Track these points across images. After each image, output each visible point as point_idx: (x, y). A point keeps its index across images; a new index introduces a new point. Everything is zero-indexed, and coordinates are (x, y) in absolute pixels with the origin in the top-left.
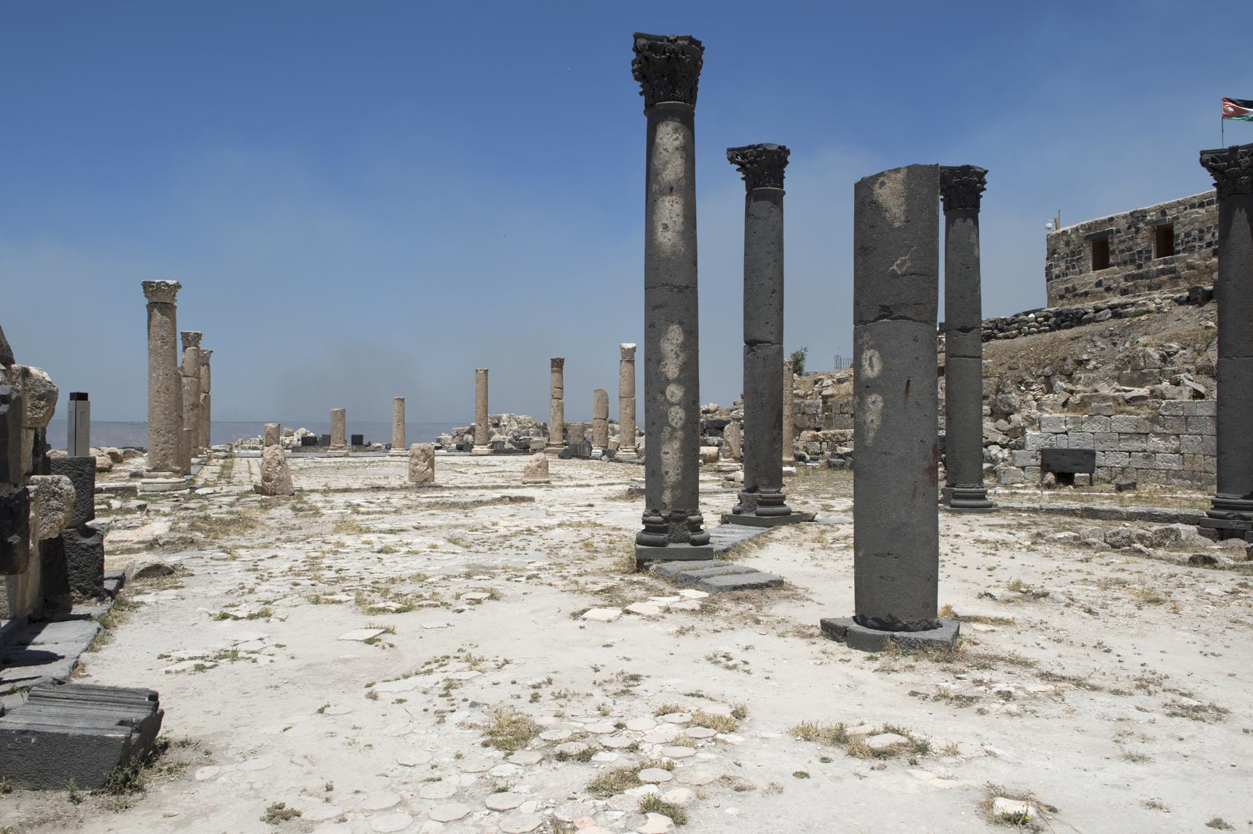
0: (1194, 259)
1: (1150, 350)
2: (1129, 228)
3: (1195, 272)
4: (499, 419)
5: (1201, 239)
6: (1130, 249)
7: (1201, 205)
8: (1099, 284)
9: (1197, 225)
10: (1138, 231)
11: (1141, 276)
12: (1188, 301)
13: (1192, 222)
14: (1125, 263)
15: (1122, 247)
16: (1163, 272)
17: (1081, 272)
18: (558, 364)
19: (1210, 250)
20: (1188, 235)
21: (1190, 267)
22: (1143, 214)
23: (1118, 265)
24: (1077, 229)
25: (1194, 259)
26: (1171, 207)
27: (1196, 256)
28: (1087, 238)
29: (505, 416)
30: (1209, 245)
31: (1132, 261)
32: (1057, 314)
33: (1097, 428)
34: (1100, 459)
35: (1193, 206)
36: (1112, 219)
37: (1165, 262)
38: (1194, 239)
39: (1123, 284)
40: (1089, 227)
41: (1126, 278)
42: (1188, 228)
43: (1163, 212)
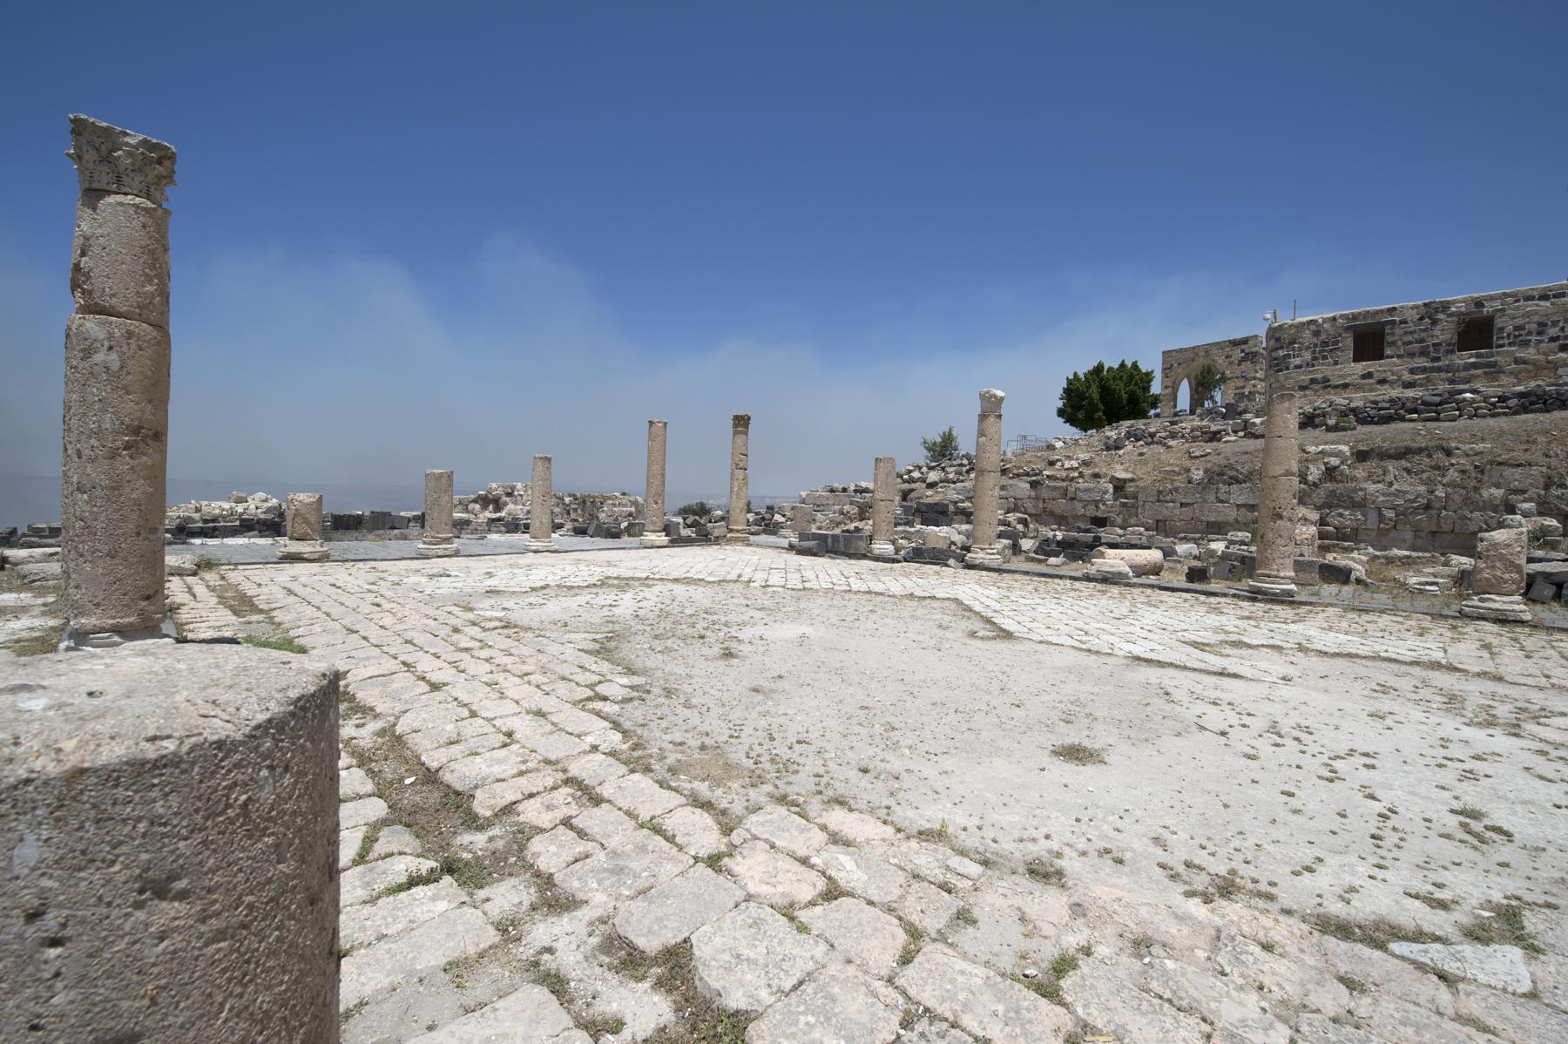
0: (1530, 353)
2: (1422, 318)
3: (1530, 367)
4: (513, 488)
5: (1539, 333)
6: (1422, 341)
7: (1544, 297)
8: (1364, 377)
9: (1536, 318)
10: (1435, 322)
11: (1439, 370)
13: (1528, 315)
14: (1412, 355)
15: (1410, 338)
16: (1474, 366)
17: (1336, 363)
18: (742, 422)
19: (1555, 345)
20: (1516, 328)
22: (1445, 306)
23: (1399, 357)
24: (1334, 319)
26: (1491, 298)
27: (1532, 350)
28: (1348, 328)
29: (519, 485)
30: (1553, 339)
31: (1424, 353)
32: (1521, 395)
35: (1530, 298)
36: (1394, 309)
37: (1478, 356)
38: (1530, 333)
39: (1407, 377)
40: (1355, 317)
41: (1412, 371)
42: (1519, 322)
43: (1479, 304)
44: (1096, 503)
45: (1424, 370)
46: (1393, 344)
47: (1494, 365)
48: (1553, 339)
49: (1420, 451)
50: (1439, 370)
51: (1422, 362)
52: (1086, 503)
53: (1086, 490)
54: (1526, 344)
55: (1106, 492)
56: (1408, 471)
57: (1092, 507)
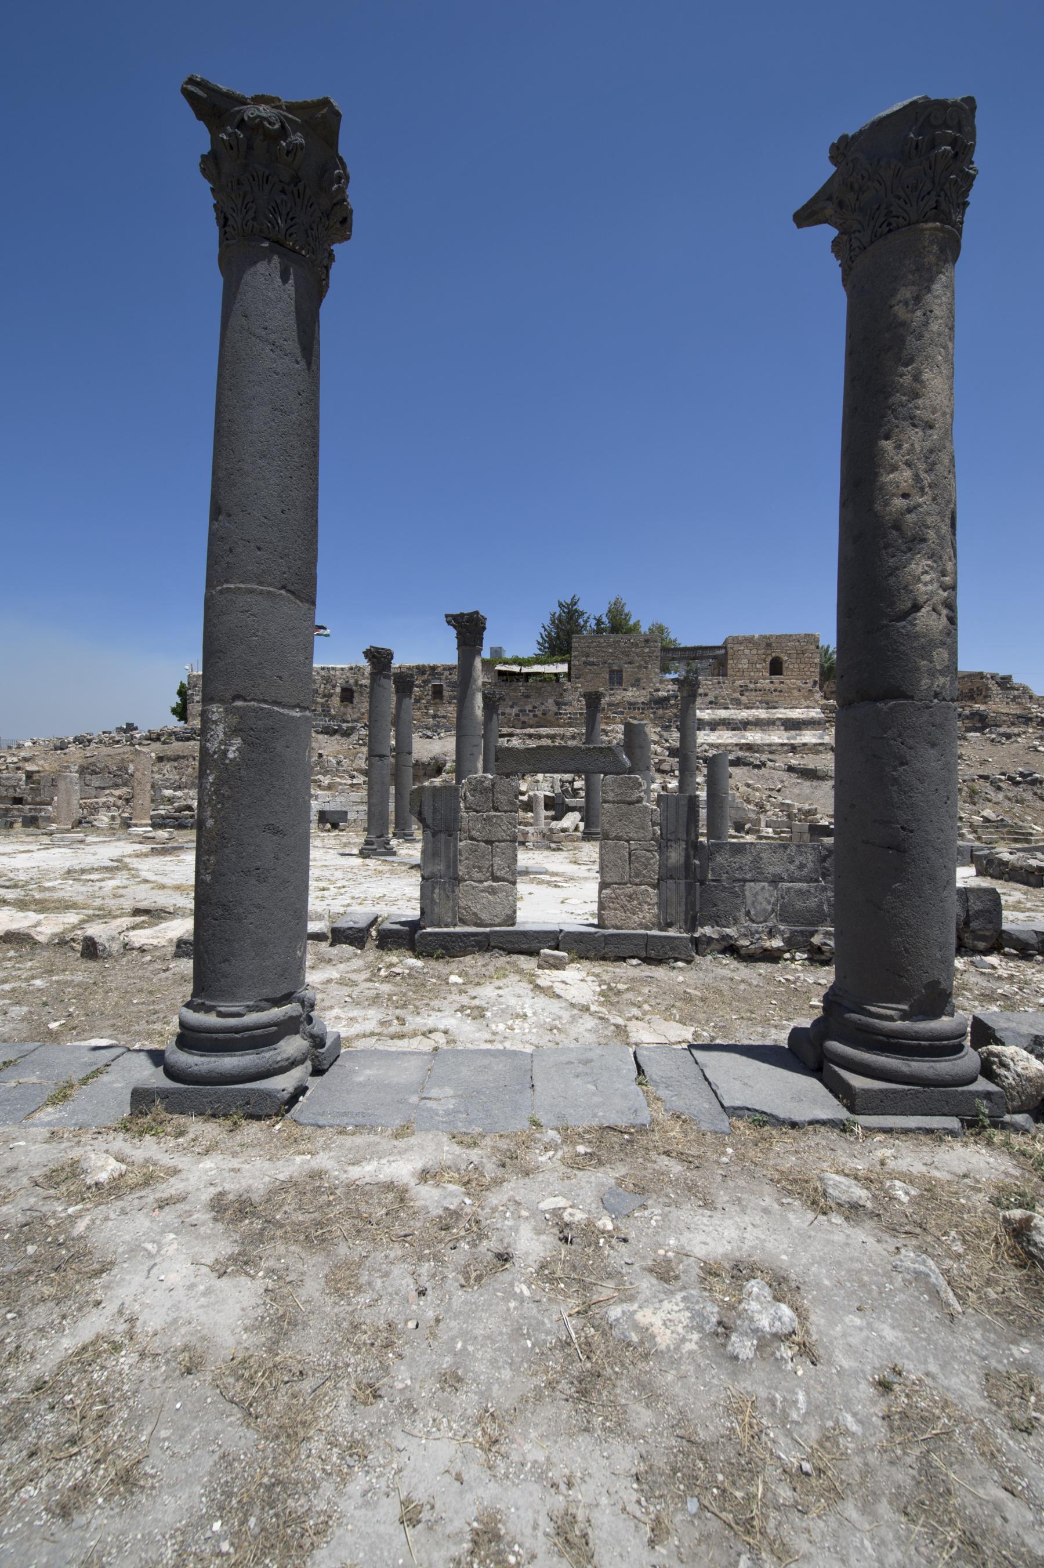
1: (331, 758)
12: (322, 733)
33: (343, 799)
34: (349, 817)
44: (14, 787)
49: (184, 757)
52: (7, 788)
53: (7, 779)
55: (20, 780)
56: (175, 768)
57: (11, 790)
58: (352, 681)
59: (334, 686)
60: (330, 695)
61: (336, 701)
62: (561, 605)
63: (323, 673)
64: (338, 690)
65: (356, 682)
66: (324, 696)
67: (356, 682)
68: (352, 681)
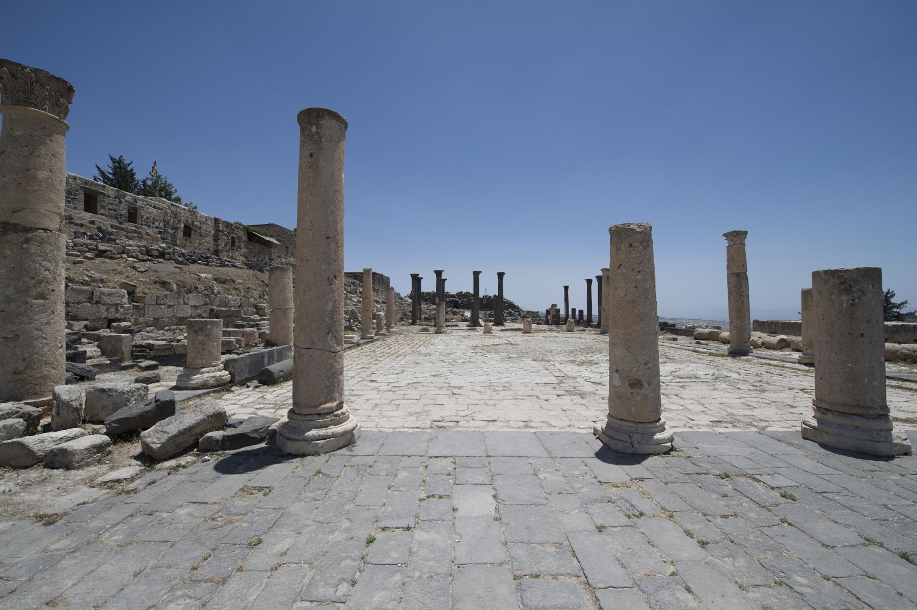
0: (150, 231)
6: (115, 210)
7: (154, 207)
13: (150, 213)
14: (111, 217)
15: (110, 206)
16: (134, 231)
17: (75, 208)
20: (148, 218)
21: (148, 234)
24: (75, 178)
25: (150, 231)
28: (82, 188)
30: (157, 228)
31: (116, 218)
41: (112, 226)
42: (148, 215)
44: (116, 305)
45: (117, 228)
46: (103, 207)
47: (140, 233)
48: (157, 228)
50: (122, 229)
51: (115, 222)
52: (109, 306)
53: (110, 295)
54: (149, 226)
55: (123, 297)
57: (113, 310)
58: (190, 221)
59: (179, 222)
60: (177, 229)
61: (180, 234)
62: (113, 160)
63: (172, 208)
64: (182, 225)
65: (193, 222)
66: (173, 228)
67: (193, 222)
68: (190, 221)
